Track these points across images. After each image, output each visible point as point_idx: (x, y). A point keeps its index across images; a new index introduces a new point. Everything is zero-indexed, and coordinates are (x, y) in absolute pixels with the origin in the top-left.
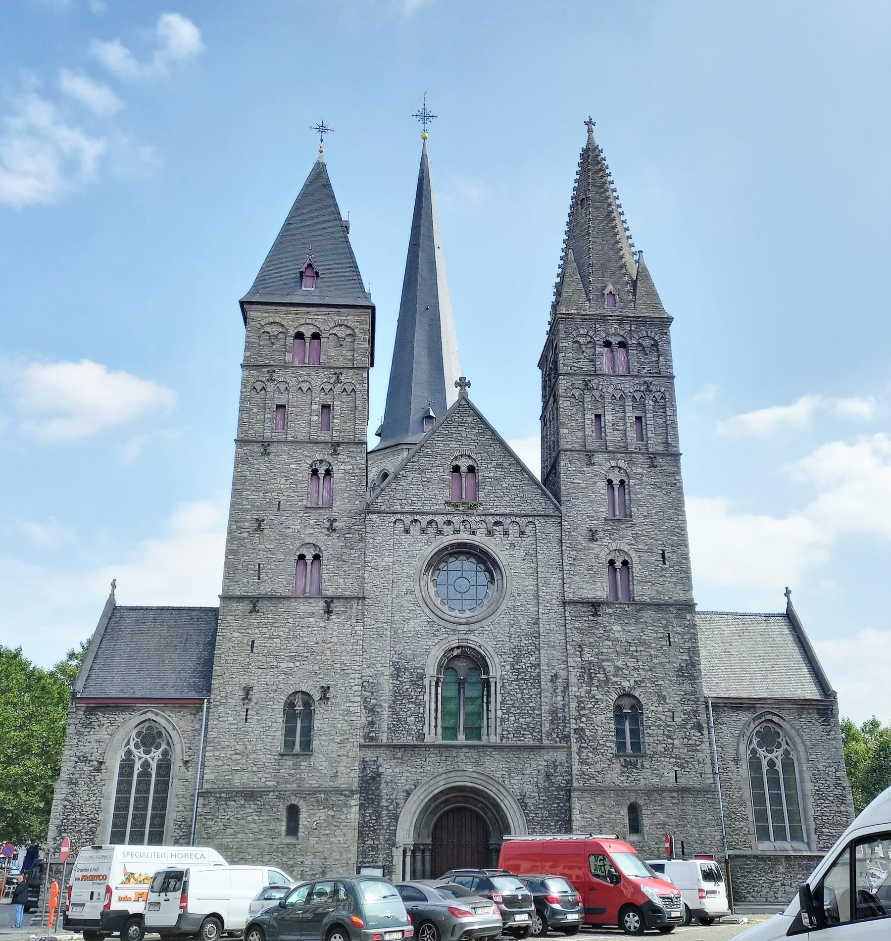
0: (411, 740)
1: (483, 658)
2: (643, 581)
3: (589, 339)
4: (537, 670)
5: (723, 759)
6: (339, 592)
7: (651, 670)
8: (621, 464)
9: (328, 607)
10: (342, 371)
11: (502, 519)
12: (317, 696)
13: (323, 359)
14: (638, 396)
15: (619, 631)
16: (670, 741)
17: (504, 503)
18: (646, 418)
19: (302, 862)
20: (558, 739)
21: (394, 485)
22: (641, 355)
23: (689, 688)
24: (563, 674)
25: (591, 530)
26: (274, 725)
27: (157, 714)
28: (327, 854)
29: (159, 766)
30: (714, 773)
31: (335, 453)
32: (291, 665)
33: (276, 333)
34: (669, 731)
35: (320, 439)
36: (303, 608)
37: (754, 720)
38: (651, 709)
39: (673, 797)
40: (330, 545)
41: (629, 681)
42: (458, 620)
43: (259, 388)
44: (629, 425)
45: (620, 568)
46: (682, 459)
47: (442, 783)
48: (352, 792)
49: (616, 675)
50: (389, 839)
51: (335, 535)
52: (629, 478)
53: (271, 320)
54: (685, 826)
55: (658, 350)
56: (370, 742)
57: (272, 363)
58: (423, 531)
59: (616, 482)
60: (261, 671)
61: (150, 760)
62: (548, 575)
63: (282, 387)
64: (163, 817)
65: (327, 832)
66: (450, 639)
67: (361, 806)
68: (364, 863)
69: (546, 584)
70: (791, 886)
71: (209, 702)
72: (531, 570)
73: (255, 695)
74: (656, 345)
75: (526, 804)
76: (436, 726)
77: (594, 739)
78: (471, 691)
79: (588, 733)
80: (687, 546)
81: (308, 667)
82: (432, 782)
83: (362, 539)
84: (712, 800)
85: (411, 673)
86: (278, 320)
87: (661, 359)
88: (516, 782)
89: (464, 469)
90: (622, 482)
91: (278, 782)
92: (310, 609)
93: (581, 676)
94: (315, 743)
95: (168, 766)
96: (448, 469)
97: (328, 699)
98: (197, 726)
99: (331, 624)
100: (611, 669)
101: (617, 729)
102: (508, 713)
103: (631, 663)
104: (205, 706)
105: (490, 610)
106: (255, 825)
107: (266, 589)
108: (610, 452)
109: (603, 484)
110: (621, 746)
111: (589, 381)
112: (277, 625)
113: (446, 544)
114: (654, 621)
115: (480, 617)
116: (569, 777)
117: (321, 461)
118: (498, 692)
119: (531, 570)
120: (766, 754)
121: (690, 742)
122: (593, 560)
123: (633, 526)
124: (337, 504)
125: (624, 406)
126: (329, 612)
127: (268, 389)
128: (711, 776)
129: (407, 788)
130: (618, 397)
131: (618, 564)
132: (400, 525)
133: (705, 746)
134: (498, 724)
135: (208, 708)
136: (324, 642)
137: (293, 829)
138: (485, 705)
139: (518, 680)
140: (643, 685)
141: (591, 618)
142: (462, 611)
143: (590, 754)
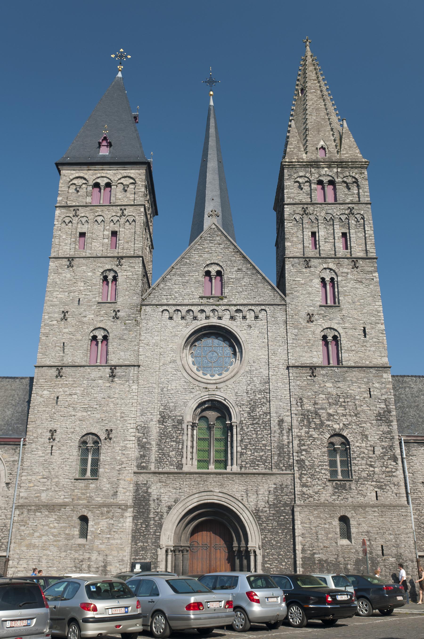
0: (173, 469)
2: (349, 350)
3: (307, 179)
4: (268, 417)
5: (414, 483)
6: (121, 362)
7: (356, 415)
8: (331, 266)
9: (112, 372)
10: (126, 207)
14: (343, 217)
15: (331, 387)
16: (372, 469)
17: (243, 296)
19: (89, 558)
20: (284, 468)
21: (162, 286)
22: (346, 190)
23: (386, 429)
25: (309, 314)
26: (71, 457)
28: (108, 552)
30: (407, 493)
31: (120, 264)
32: (85, 414)
33: (80, 184)
34: (371, 461)
35: (109, 255)
36: (95, 373)
38: (356, 444)
39: (374, 511)
41: (339, 424)
42: (209, 381)
43: (67, 221)
44: (336, 238)
45: (331, 341)
47: (196, 500)
49: (329, 420)
50: (155, 542)
51: (119, 322)
52: (337, 276)
53: (77, 175)
54: (384, 533)
56: (142, 468)
58: (183, 318)
59: (328, 279)
60: (62, 418)
62: (276, 347)
65: (108, 536)
67: (135, 518)
68: (136, 559)
69: (274, 354)
71: (25, 440)
72: (263, 344)
73: (57, 436)
75: (260, 516)
76: (192, 459)
77: (312, 466)
78: (217, 433)
79: (307, 463)
82: (188, 499)
84: (405, 514)
86: (82, 175)
87: (361, 191)
88: (252, 500)
89: (213, 273)
90: (332, 279)
91: (73, 499)
93: (302, 421)
94: (101, 470)
96: (202, 273)
97: (110, 439)
98: (17, 458)
99: (114, 385)
101: (330, 460)
102: (246, 448)
103: (341, 411)
105: (232, 374)
107: (68, 360)
108: (323, 258)
109: (317, 282)
110: (334, 473)
111: (307, 208)
112: (75, 385)
113: (200, 326)
115: (225, 379)
117: (110, 270)
119: (263, 344)
121: (387, 470)
122: (311, 336)
123: (341, 310)
124: (120, 300)
126: (113, 376)
127: (74, 222)
128: (405, 495)
130: (328, 219)
132: (166, 315)
134: (239, 456)
135: (24, 445)
136: (109, 397)
137: (84, 534)
139: (253, 424)
140: (350, 427)
141: (309, 378)
142: (212, 376)
143: (309, 479)
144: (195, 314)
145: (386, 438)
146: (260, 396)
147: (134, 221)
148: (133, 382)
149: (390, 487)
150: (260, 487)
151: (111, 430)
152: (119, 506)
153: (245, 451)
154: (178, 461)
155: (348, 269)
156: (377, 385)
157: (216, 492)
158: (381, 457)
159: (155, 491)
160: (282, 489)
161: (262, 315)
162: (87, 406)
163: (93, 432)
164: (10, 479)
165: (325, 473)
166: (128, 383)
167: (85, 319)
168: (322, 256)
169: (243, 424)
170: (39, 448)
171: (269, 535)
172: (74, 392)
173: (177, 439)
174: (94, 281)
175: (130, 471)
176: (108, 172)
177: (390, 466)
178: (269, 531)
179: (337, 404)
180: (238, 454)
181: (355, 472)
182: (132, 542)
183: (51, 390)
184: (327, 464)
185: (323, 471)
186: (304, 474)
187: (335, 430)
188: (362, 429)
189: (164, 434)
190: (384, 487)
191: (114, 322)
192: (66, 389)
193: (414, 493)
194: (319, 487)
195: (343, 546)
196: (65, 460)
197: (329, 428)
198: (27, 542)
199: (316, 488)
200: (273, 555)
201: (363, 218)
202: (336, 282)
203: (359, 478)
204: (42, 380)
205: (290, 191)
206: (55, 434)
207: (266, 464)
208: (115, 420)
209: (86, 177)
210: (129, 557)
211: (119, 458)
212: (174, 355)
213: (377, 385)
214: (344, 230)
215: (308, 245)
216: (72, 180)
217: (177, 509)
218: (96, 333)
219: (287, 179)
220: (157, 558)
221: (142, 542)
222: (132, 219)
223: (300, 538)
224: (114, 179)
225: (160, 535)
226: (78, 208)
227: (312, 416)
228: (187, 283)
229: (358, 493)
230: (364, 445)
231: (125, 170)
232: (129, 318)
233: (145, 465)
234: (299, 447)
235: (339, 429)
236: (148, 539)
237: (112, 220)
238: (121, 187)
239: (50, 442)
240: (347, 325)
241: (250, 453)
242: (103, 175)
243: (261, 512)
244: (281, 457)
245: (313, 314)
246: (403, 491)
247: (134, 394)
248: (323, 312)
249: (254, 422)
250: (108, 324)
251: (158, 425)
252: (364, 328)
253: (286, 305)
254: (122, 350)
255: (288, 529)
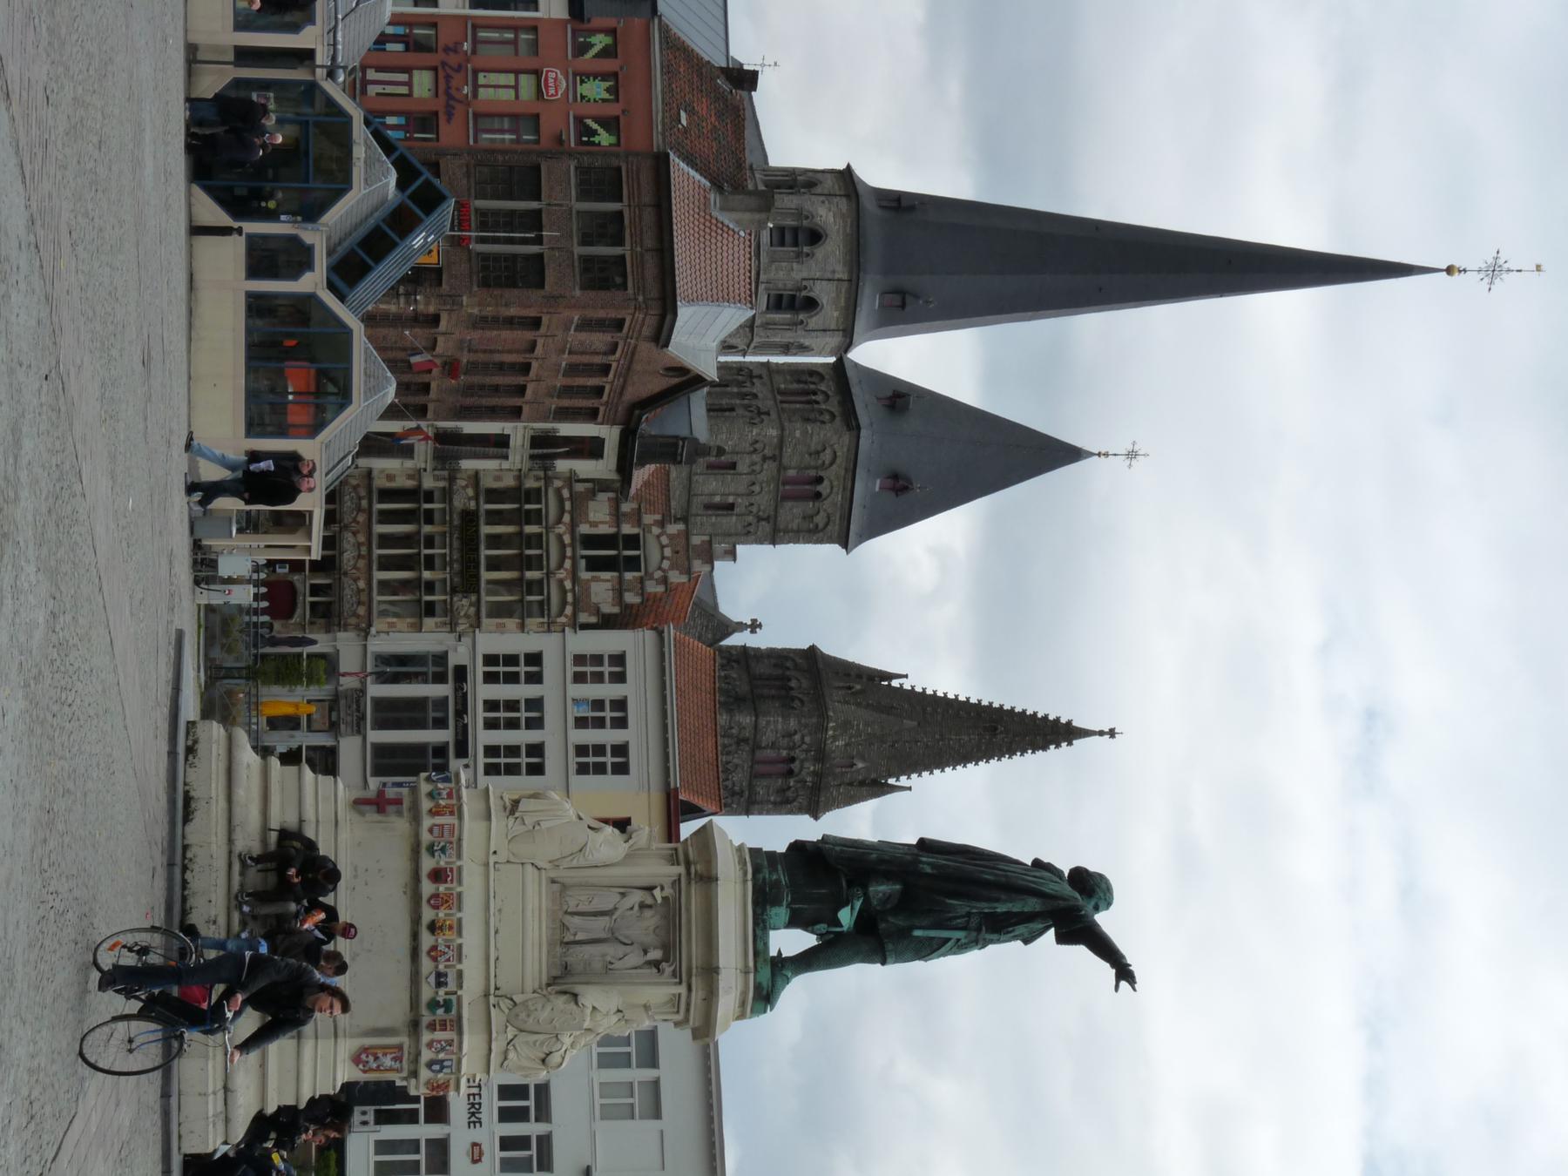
13: (789, 504)
63: (757, 468)
86: (838, 461)
224: (826, 505)
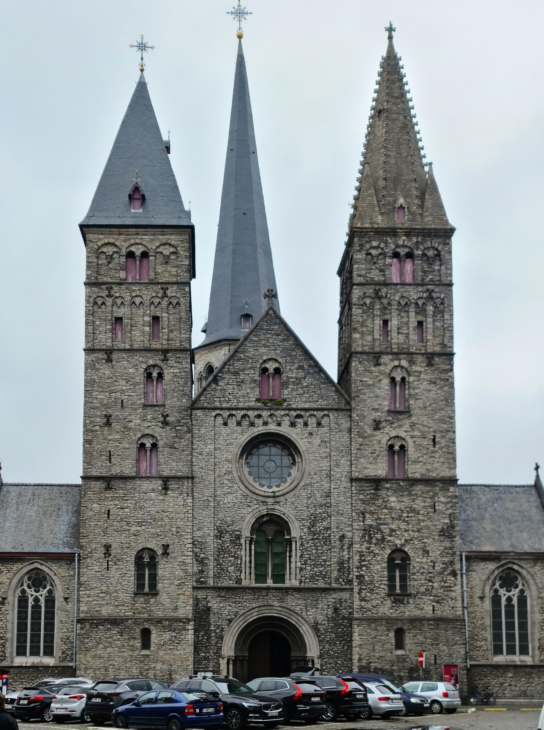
0: (231, 583)
1: (287, 523)
2: (416, 462)
3: (380, 251)
6: (173, 473)
7: (418, 531)
8: (404, 363)
9: (165, 484)
10: (168, 286)
11: (302, 413)
12: (160, 552)
14: (420, 302)
15: (394, 502)
16: (430, 584)
17: (304, 399)
18: (426, 321)
19: (154, 667)
20: (343, 583)
23: (448, 544)
24: (349, 535)
25: (375, 421)
26: (129, 572)
27: (42, 564)
28: (172, 662)
29: (46, 601)
30: (463, 607)
31: (165, 359)
32: (139, 528)
33: (111, 253)
34: (430, 577)
36: (146, 485)
37: (498, 568)
39: (430, 624)
40: (163, 435)
41: (400, 539)
43: (100, 303)
44: (411, 329)
46: (456, 359)
47: (255, 614)
48: (189, 620)
49: (390, 536)
50: (217, 652)
51: (168, 428)
55: (440, 260)
56: (200, 586)
57: (110, 280)
58: (239, 424)
59: (398, 379)
60: (116, 533)
61: (40, 597)
62: (339, 458)
63: (119, 301)
64: (53, 636)
65: (171, 647)
66: (261, 509)
67: (195, 630)
69: (338, 465)
70: (516, 686)
73: (113, 552)
74: (439, 255)
75: (319, 629)
76: (250, 574)
77: (372, 582)
79: (367, 578)
80: (454, 432)
81: (152, 530)
82: (248, 613)
83: (190, 431)
85: (231, 534)
86: (112, 241)
90: (403, 379)
91: (134, 613)
92: (152, 486)
93: (363, 537)
94: (160, 586)
95: (53, 601)
97: (168, 554)
98: (72, 573)
100: (387, 531)
102: (305, 564)
103: (403, 526)
104: (76, 558)
105: (292, 486)
106: (119, 642)
107: (116, 470)
109: (386, 381)
110: (392, 587)
111: (379, 290)
112: (126, 498)
114: (423, 493)
115: (284, 491)
116: (351, 610)
117: (154, 366)
118: (298, 548)
119: (326, 455)
120: (505, 593)
121: (446, 585)
123: (410, 416)
125: (407, 312)
126: (166, 488)
127: (108, 304)
128: (461, 609)
129: (229, 617)
131: (397, 448)
132: (220, 420)
133: (458, 588)
136: (163, 511)
138: (288, 558)
139: (313, 539)
140: (412, 542)
143: (368, 594)
144: (252, 419)
145: (447, 553)
146: (320, 511)
147: (178, 303)
148: (188, 496)
149: (447, 601)
150: (319, 602)
151: (168, 546)
152: (180, 620)
153: (304, 566)
154: (237, 576)
155: (422, 367)
156: (442, 499)
157: (275, 606)
158: (441, 573)
159: (214, 605)
160: (341, 603)
161: (324, 421)
162: (140, 520)
163: (149, 546)
164: (68, 594)
165: (384, 588)
166: (182, 496)
167: (130, 425)
168: (394, 351)
169: (302, 539)
170: (95, 563)
171: (327, 647)
172: (125, 505)
173: (235, 554)
174: (137, 379)
175: (190, 586)
176: (144, 237)
177: (449, 581)
178: (328, 642)
179: (400, 519)
180: (298, 569)
181: (414, 587)
182: (194, 652)
183: (101, 503)
184: (386, 579)
185: (382, 586)
186: (363, 589)
187: (396, 545)
188: (423, 544)
189: (222, 549)
190: (442, 601)
191: (162, 428)
192: (117, 502)
193: (470, 607)
194: (377, 602)
195: (398, 655)
196: (123, 575)
197: (390, 544)
198: (92, 653)
199: (374, 603)
200: (330, 664)
201: (442, 303)
202: (407, 383)
203: (418, 593)
204: (91, 493)
205: (361, 266)
206: (110, 549)
207: (326, 579)
208: (170, 535)
209: (117, 243)
210: (193, 666)
211: (177, 573)
212: (230, 466)
213: (442, 499)
214: (420, 318)
215: (378, 337)
216: (100, 248)
217: (238, 622)
218: (144, 441)
219: (358, 251)
220: (219, 667)
221: (204, 653)
222: (176, 301)
223: (357, 648)
224: (152, 246)
225: (221, 646)
226: (111, 286)
227: (374, 531)
228: (243, 382)
229: (416, 607)
230: (424, 560)
231: (164, 235)
232: (180, 424)
233: (204, 580)
234: (360, 562)
235: (400, 544)
236: (210, 650)
237: (152, 302)
238: (160, 259)
239: (105, 557)
240: (416, 433)
241: (309, 568)
242: (137, 241)
243: (320, 625)
244: (341, 572)
245: (380, 421)
246: (459, 604)
247: (190, 508)
248: (391, 418)
249: (315, 537)
250: (158, 431)
251: (215, 540)
252: (434, 437)
253: (351, 410)
254: (173, 460)
255: (346, 640)
